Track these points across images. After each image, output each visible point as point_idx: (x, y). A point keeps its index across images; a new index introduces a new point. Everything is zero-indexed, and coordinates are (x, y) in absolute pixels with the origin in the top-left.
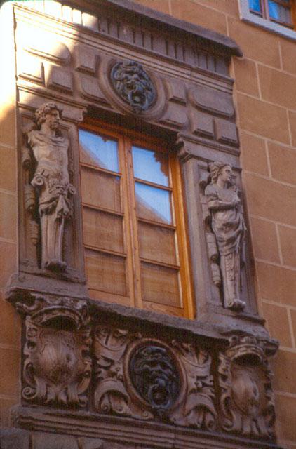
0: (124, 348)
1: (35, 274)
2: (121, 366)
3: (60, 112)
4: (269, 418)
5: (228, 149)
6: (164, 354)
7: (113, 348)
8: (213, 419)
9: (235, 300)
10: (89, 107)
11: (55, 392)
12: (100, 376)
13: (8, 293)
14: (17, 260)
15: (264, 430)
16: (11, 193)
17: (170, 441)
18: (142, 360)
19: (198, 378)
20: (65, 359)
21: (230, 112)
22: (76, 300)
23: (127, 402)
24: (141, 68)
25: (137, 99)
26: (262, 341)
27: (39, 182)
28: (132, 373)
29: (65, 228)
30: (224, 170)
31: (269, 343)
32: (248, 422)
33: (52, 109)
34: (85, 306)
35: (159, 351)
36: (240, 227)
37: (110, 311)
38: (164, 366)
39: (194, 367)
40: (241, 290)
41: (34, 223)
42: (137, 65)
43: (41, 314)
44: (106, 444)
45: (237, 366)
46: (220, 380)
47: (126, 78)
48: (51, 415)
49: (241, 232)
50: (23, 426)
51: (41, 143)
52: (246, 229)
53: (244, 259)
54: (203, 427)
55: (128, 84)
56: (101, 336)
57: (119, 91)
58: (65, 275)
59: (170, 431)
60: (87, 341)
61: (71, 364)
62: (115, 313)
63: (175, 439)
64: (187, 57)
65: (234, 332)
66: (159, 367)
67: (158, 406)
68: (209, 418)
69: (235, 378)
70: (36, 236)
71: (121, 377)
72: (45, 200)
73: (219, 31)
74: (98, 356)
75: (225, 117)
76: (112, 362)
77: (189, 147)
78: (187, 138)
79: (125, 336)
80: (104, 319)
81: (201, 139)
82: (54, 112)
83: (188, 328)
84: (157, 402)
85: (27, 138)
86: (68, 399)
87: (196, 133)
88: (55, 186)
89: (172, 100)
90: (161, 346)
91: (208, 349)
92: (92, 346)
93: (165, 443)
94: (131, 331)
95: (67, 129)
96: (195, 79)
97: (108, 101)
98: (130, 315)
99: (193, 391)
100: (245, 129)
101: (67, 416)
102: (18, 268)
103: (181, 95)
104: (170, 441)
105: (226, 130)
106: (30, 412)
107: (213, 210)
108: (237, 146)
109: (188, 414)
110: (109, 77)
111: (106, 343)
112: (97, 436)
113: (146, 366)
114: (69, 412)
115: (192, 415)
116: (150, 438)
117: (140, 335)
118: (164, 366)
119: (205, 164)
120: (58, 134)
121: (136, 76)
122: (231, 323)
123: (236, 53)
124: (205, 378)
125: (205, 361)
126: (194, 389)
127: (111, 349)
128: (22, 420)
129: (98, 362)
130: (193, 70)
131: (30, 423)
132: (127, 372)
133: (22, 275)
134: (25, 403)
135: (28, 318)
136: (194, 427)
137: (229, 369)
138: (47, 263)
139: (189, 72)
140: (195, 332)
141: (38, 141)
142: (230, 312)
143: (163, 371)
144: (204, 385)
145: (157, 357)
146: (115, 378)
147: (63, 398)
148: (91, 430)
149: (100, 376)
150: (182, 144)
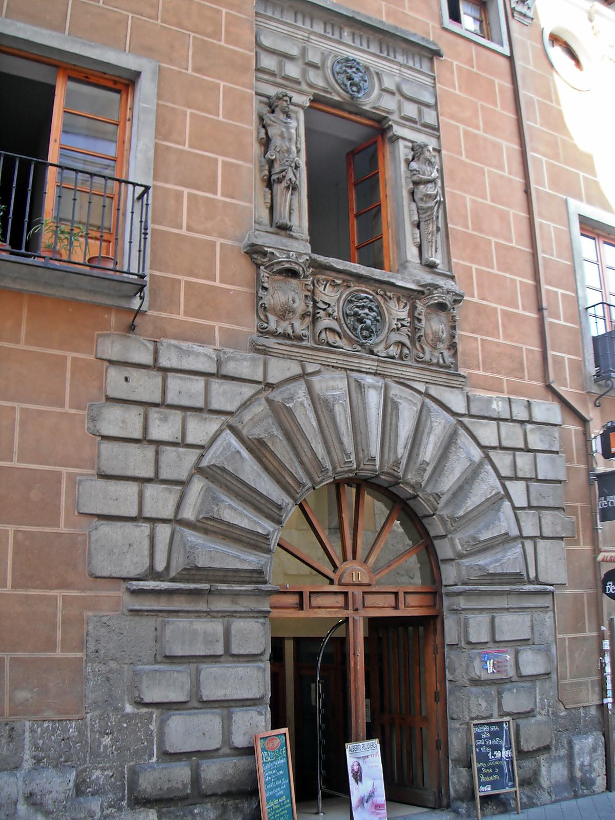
0: (338, 294)
1: (266, 232)
2: (336, 309)
3: (291, 98)
4: (452, 352)
6: (371, 301)
7: (330, 294)
8: (408, 352)
9: (431, 259)
10: (315, 95)
11: (284, 327)
12: (318, 315)
13: (245, 247)
17: (374, 368)
18: (353, 305)
19: (398, 320)
21: (431, 101)
23: (340, 337)
24: (358, 63)
25: (355, 89)
29: (292, 194)
31: (457, 294)
32: (436, 354)
33: (284, 96)
34: (307, 260)
35: (368, 298)
36: (438, 198)
37: (327, 264)
38: (371, 309)
40: (436, 251)
42: (355, 61)
43: (272, 265)
44: (323, 368)
45: (429, 311)
46: (416, 322)
48: (279, 344)
49: (439, 203)
50: (258, 351)
51: (274, 124)
52: (442, 199)
53: (440, 225)
57: (339, 81)
58: (291, 233)
59: (373, 360)
60: (309, 288)
61: (295, 305)
62: (333, 266)
63: (377, 366)
65: (429, 285)
66: (367, 311)
67: (364, 341)
70: (269, 201)
72: (277, 171)
73: (424, 36)
75: (428, 106)
76: (329, 305)
77: (397, 130)
79: (339, 285)
81: (407, 123)
83: (392, 280)
84: (365, 338)
85: (263, 120)
86: (293, 332)
88: (285, 159)
90: (371, 295)
91: (409, 298)
92: (313, 293)
94: (344, 281)
95: (296, 113)
97: (329, 90)
98: (345, 268)
101: (293, 346)
103: (392, 87)
104: (374, 368)
105: (429, 117)
106: (263, 341)
107: (416, 183)
108: (438, 130)
110: (332, 70)
112: (316, 362)
113: (356, 309)
114: (295, 343)
115: (391, 348)
116: (357, 365)
118: (371, 309)
119: (410, 145)
120: (288, 117)
121: (354, 70)
122: (428, 278)
123: (437, 54)
124: (403, 320)
126: (394, 329)
128: (258, 347)
129: (318, 305)
130: (401, 65)
131: (265, 350)
132: (341, 313)
133: (257, 233)
134: (260, 334)
135: (262, 267)
136: (393, 358)
137: (423, 314)
138: (277, 223)
139: (399, 68)
140: (397, 284)
141: (272, 123)
142: (427, 269)
143: (370, 313)
144: (403, 326)
145: (365, 302)
147: (290, 331)
148: (310, 357)
149: (318, 315)
150: (391, 127)
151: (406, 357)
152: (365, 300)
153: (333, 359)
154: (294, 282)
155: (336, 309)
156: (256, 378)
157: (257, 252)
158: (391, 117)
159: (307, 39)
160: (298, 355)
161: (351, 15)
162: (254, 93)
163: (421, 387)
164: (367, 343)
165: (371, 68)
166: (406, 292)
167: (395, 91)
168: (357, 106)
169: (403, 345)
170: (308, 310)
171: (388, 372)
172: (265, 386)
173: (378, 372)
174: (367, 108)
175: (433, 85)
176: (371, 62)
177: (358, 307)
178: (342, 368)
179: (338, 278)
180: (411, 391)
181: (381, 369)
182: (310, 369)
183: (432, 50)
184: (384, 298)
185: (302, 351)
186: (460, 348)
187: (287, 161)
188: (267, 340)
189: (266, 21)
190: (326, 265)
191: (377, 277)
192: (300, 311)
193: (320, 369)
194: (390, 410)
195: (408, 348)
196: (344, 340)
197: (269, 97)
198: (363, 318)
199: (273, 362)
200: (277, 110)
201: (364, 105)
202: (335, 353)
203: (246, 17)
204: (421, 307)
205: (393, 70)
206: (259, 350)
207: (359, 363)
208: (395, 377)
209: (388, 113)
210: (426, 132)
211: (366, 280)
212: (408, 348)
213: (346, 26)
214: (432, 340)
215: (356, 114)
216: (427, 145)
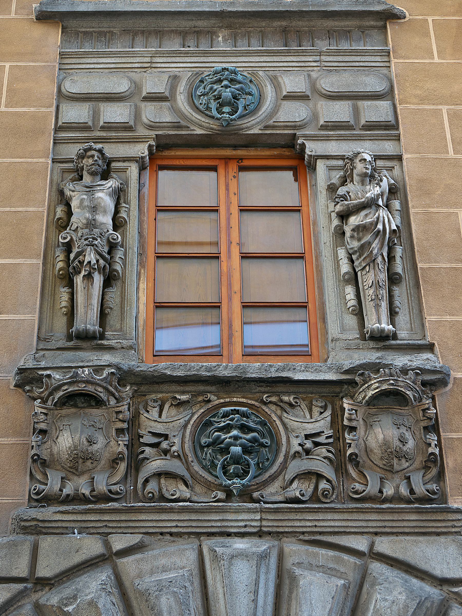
1: (58, 349)
3: (100, 151)
4: (434, 471)
5: (377, 135)
6: (244, 415)
8: (328, 486)
12: (141, 456)
14: (36, 335)
15: (420, 489)
16: (34, 261)
19: (307, 437)
20: (85, 442)
22: (98, 369)
23: (186, 485)
24: (235, 73)
26: (413, 370)
27: (65, 238)
28: (198, 447)
30: (357, 161)
33: (86, 150)
35: (237, 412)
37: (156, 374)
38: (244, 428)
39: (304, 423)
41: (66, 289)
44: (147, 539)
47: (211, 88)
54: (315, 498)
55: (215, 96)
56: (149, 408)
57: (201, 107)
59: (250, 511)
61: (95, 447)
62: (165, 374)
63: (261, 520)
64: (317, 41)
65: (362, 366)
67: (230, 482)
68: (323, 485)
69: (369, 426)
71: (176, 454)
74: (141, 432)
76: (166, 437)
77: (312, 148)
78: (307, 137)
80: (147, 384)
82: (89, 153)
83: (284, 374)
86: (93, 490)
87: (324, 127)
88: (83, 238)
89: (286, 98)
93: (246, 526)
94: (196, 395)
96: (326, 64)
97: (183, 123)
99: (297, 455)
100: (407, 103)
102: (35, 346)
105: (377, 111)
106: (35, 513)
107: (344, 216)
109: (292, 481)
111: (160, 416)
113: (216, 433)
115: (295, 485)
116: (219, 524)
117: (213, 397)
121: (225, 82)
123: (390, 16)
124: (318, 434)
125: (321, 413)
126: (298, 452)
127: (167, 421)
128: (23, 524)
129: (141, 440)
132: (187, 446)
139: (317, 58)
142: (372, 344)
144: (317, 444)
145: (232, 420)
146: (168, 457)
149: (141, 456)
150: (303, 146)
151: (326, 496)
152: (231, 416)
153: (169, 521)
154: (96, 413)
155: (176, 440)
156: (15, 573)
157: (30, 382)
158: (298, 133)
159: (148, 65)
160: (99, 525)
161: (218, 10)
162: (50, 162)
163: (361, 544)
164: (234, 483)
165: (260, 73)
166: (326, 390)
167: (308, 93)
168: (236, 133)
169: (319, 476)
170: (120, 449)
171: (286, 526)
172: (35, 584)
173: (265, 529)
174: (256, 131)
175: (387, 64)
176: (264, 64)
177: (220, 430)
178: (189, 534)
179: (183, 393)
180: (331, 553)
181: (270, 524)
182: (119, 543)
183: (377, 13)
184: (280, 406)
185: (107, 517)
186: (450, 462)
187: (86, 239)
188: (42, 509)
189: (78, 61)
190: (154, 377)
191: (254, 376)
192: (106, 456)
193: (141, 542)
194: (287, 592)
195: (328, 480)
196: (198, 489)
197: (71, 161)
198: (230, 445)
199: (47, 543)
200: (85, 173)
201: (248, 128)
202: (171, 510)
203: (43, 64)
204: (351, 407)
205: (307, 64)
206: (25, 528)
207: (223, 520)
208: (303, 533)
209: (294, 127)
210: (370, 135)
211: (240, 384)
212: (328, 480)
213: (221, 27)
214: (382, 459)
215: (246, 146)
216: (359, 153)
